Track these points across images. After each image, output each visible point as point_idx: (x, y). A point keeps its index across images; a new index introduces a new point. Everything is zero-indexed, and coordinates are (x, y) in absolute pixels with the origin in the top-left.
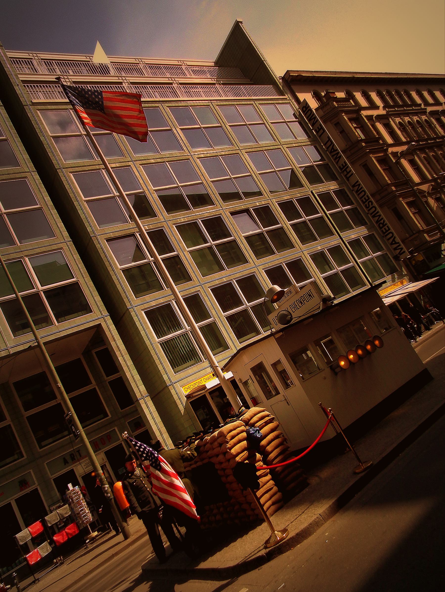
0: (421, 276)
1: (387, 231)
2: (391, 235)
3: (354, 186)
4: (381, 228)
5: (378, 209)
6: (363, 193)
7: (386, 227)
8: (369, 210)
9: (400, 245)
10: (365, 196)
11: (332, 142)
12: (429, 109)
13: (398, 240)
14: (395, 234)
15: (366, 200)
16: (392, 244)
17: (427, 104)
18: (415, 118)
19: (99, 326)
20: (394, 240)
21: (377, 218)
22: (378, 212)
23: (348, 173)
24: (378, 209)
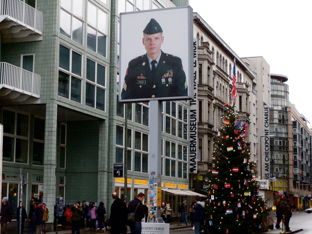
0: (194, 190)
1: (193, 151)
2: (194, 155)
3: (191, 111)
4: (191, 147)
5: (196, 135)
6: (194, 119)
8: (191, 132)
9: (195, 164)
10: (194, 123)
13: (196, 160)
14: (196, 156)
15: (193, 125)
16: (191, 160)
17: (230, 78)
18: (223, 84)
19: (105, 120)
20: (194, 159)
21: (192, 139)
22: (196, 137)
24: (196, 135)
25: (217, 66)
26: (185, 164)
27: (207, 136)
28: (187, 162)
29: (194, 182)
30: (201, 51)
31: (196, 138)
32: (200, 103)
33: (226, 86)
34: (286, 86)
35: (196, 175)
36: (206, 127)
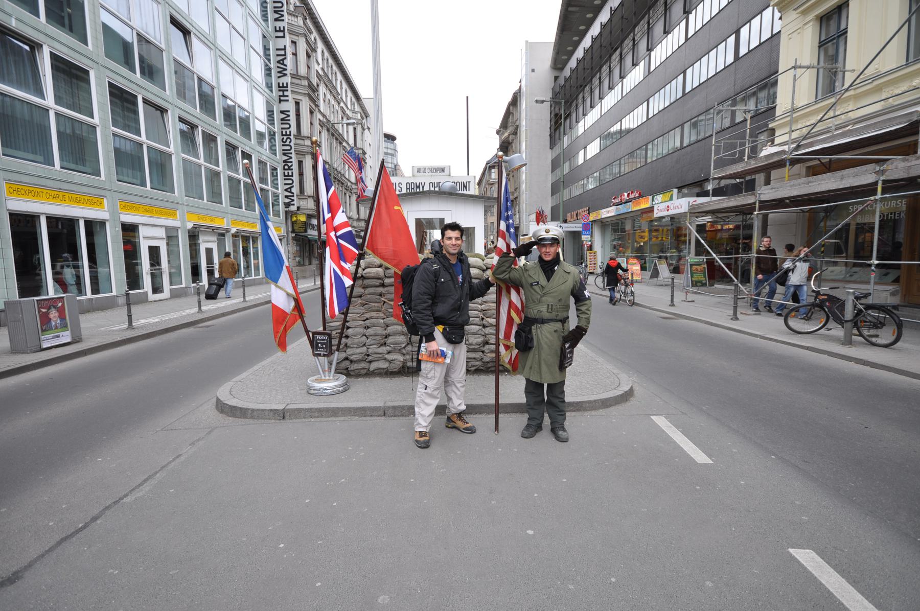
1: (288, 176)
2: (290, 182)
3: (282, 112)
6: (287, 126)
7: (290, 172)
11: (285, 55)
12: (342, 104)
13: (293, 190)
15: (286, 135)
16: (286, 190)
18: (333, 102)
20: (290, 188)
21: (286, 158)
23: (284, 96)
24: (292, 151)
25: (323, 69)
26: (276, 196)
27: (310, 157)
28: (280, 191)
29: (293, 223)
30: (293, 18)
31: (293, 155)
32: (297, 104)
33: (337, 107)
34: (395, 145)
35: (293, 214)
36: (308, 142)
